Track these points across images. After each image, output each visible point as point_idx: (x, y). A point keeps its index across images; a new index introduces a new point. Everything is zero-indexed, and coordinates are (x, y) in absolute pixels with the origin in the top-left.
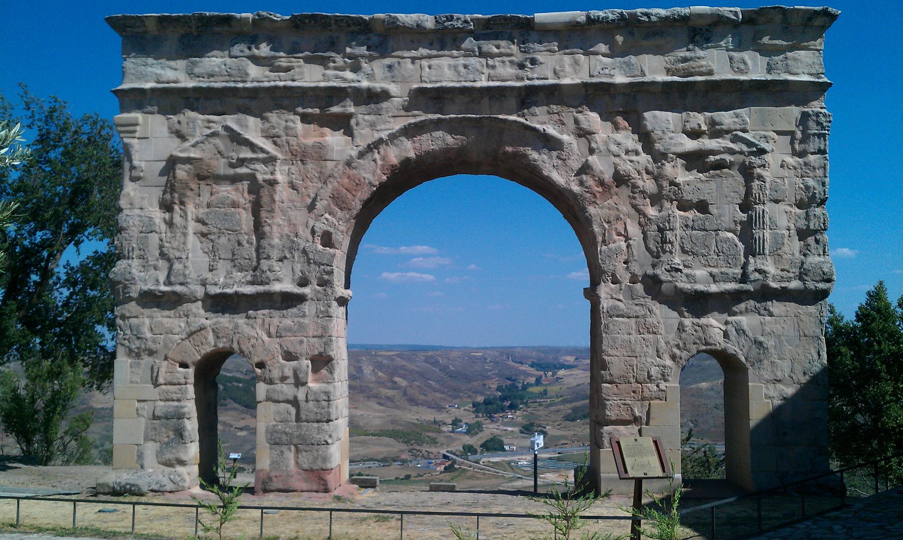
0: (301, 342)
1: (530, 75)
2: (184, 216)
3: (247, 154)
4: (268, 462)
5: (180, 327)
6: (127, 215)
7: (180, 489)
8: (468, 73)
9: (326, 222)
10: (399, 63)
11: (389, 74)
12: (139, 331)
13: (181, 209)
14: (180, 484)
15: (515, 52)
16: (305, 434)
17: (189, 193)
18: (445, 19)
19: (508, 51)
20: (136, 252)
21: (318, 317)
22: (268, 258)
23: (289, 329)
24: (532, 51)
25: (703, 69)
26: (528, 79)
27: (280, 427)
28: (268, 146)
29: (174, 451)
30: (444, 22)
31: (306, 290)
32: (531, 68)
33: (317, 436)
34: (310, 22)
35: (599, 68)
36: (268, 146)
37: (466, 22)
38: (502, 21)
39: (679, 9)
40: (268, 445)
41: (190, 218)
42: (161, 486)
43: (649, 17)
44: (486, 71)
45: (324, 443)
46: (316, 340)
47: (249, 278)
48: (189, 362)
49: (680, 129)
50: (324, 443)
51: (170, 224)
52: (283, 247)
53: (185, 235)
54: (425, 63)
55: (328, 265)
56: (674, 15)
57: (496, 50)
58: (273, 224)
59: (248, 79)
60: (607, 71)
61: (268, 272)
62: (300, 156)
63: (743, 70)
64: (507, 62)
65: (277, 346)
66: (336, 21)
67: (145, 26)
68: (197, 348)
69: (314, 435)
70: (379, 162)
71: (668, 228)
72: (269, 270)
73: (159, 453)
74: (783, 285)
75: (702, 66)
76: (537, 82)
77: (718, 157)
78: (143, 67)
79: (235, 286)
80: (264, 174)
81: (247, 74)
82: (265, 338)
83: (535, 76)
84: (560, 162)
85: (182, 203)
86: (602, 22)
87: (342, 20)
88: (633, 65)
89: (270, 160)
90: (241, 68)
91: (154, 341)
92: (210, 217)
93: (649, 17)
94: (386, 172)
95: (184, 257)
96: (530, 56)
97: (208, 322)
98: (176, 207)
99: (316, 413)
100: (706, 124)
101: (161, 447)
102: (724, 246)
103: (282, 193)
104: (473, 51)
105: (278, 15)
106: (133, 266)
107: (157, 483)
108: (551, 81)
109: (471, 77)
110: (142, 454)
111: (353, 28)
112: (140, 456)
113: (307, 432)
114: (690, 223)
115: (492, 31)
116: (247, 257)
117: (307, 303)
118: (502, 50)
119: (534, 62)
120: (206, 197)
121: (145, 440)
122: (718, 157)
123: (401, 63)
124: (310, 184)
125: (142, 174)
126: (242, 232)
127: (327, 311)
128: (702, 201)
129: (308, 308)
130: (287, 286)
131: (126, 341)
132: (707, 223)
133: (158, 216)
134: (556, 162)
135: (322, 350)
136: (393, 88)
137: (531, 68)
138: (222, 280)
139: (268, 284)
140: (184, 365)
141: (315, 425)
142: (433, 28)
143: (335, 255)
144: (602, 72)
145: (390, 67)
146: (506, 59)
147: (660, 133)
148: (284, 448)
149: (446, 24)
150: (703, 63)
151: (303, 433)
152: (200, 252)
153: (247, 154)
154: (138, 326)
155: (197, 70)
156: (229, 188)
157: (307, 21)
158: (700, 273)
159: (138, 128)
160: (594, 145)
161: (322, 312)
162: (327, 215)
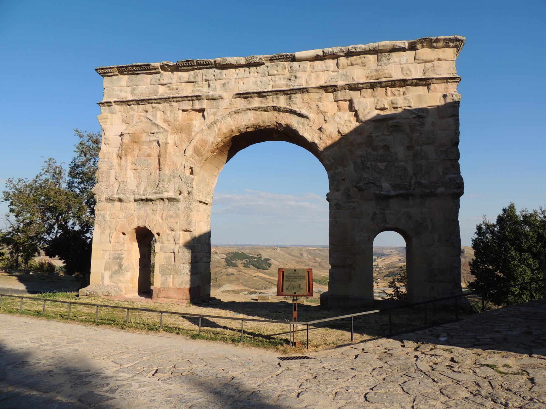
0: (177, 223)
1: (293, 84)
2: (126, 162)
3: (155, 130)
4: (160, 283)
5: (122, 215)
6: (101, 162)
7: (119, 295)
8: (262, 85)
9: (190, 162)
10: (228, 83)
11: (223, 88)
12: (104, 217)
13: (125, 158)
14: (119, 293)
15: (286, 73)
17: (129, 150)
18: (250, 58)
19: (283, 73)
20: (105, 179)
21: (185, 210)
22: (163, 181)
23: (171, 216)
24: (294, 72)
25: (387, 75)
26: (292, 86)
27: (166, 266)
28: (165, 126)
29: (117, 276)
30: (250, 60)
31: (180, 197)
32: (294, 81)
35: (330, 78)
36: (165, 126)
37: (261, 59)
38: (280, 57)
39: (372, 44)
40: (160, 275)
41: (128, 162)
42: (109, 293)
43: (356, 49)
44: (271, 83)
45: (186, 274)
46: (183, 222)
47: (154, 191)
49: (374, 107)
50: (186, 274)
51: (120, 165)
52: (170, 175)
53: (126, 170)
54: (241, 82)
55: (191, 184)
56: (369, 47)
57: (276, 72)
58: (165, 164)
59: (159, 95)
60: (334, 80)
61: (162, 188)
62: (179, 130)
63: (409, 75)
64: (282, 79)
65: (165, 224)
68: (129, 225)
70: (217, 132)
71: (366, 160)
72: (163, 186)
73: (111, 277)
74: (433, 191)
75: (385, 74)
76: (296, 87)
77: (395, 121)
78: (112, 92)
79: (148, 195)
80: (162, 139)
81: (158, 93)
82: (161, 221)
83: (296, 84)
84: (309, 128)
85: (126, 155)
86: (330, 54)
88: (348, 76)
89: (166, 131)
90: (155, 89)
91: (110, 222)
92: (138, 161)
93: (356, 49)
94: (220, 136)
95: (125, 181)
96: (294, 74)
97: (135, 212)
98: (123, 157)
99: (183, 259)
100: (388, 104)
101: (112, 274)
102: (399, 170)
103: (171, 149)
104: (265, 74)
105: (171, 63)
106: (102, 186)
107: (107, 291)
108: (304, 86)
109: (263, 87)
110: (103, 277)
112: (102, 278)
114: (379, 158)
115: (274, 63)
116: (154, 180)
117: (181, 203)
118: (279, 72)
119: (296, 77)
120: (136, 152)
121: (105, 270)
122: (395, 121)
123: (229, 82)
124: (184, 144)
125: (109, 142)
126: (152, 168)
127: (189, 207)
128: (386, 145)
129: (181, 205)
130: (171, 194)
132: (389, 158)
133: (115, 161)
134: (307, 127)
135: (187, 227)
136: (225, 95)
137: (294, 81)
138: (142, 192)
139: (161, 193)
142: (244, 63)
143: (194, 179)
144: (331, 80)
145: (224, 85)
146: (281, 76)
147: (363, 110)
148: (167, 276)
149: (251, 61)
150: (387, 72)
152: (133, 178)
153: (155, 130)
154: (104, 214)
155: (135, 92)
156: (147, 147)
158: (385, 185)
159: (108, 120)
160: (326, 118)
161: (187, 207)
162: (191, 159)
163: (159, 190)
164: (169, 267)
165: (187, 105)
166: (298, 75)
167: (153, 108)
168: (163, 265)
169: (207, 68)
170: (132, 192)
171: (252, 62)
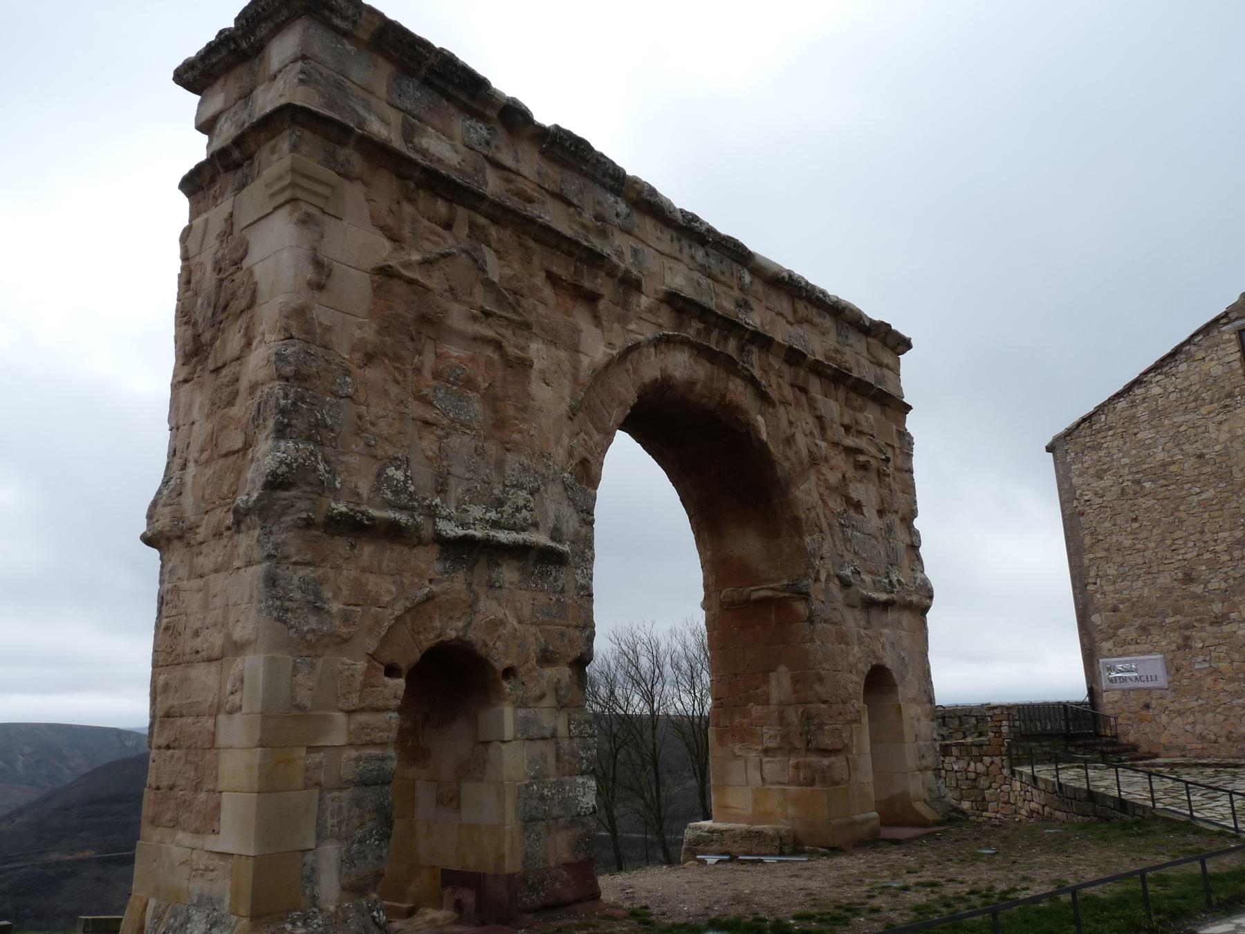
16: (569, 797)
27: (535, 787)
33: (584, 800)
34: (571, 145)
48: (404, 665)
66: (598, 161)
67: (355, 23)
69: (580, 798)
87: (605, 163)
101: (348, 850)
111: (608, 180)
113: (571, 794)
131: (289, 615)
140: (391, 671)
141: (580, 780)
151: (567, 795)
157: (568, 144)
163: (513, 515)
164: (545, 791)
165: (562, 269)
166: (753, 303)
167: (472, 226)
168: (527, 786)
169: (603, 185)
170: (429, 507)
171: (696, 230)
